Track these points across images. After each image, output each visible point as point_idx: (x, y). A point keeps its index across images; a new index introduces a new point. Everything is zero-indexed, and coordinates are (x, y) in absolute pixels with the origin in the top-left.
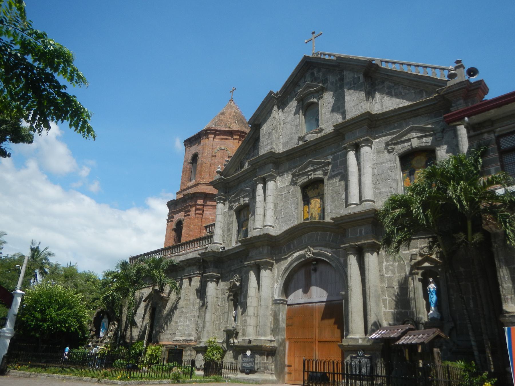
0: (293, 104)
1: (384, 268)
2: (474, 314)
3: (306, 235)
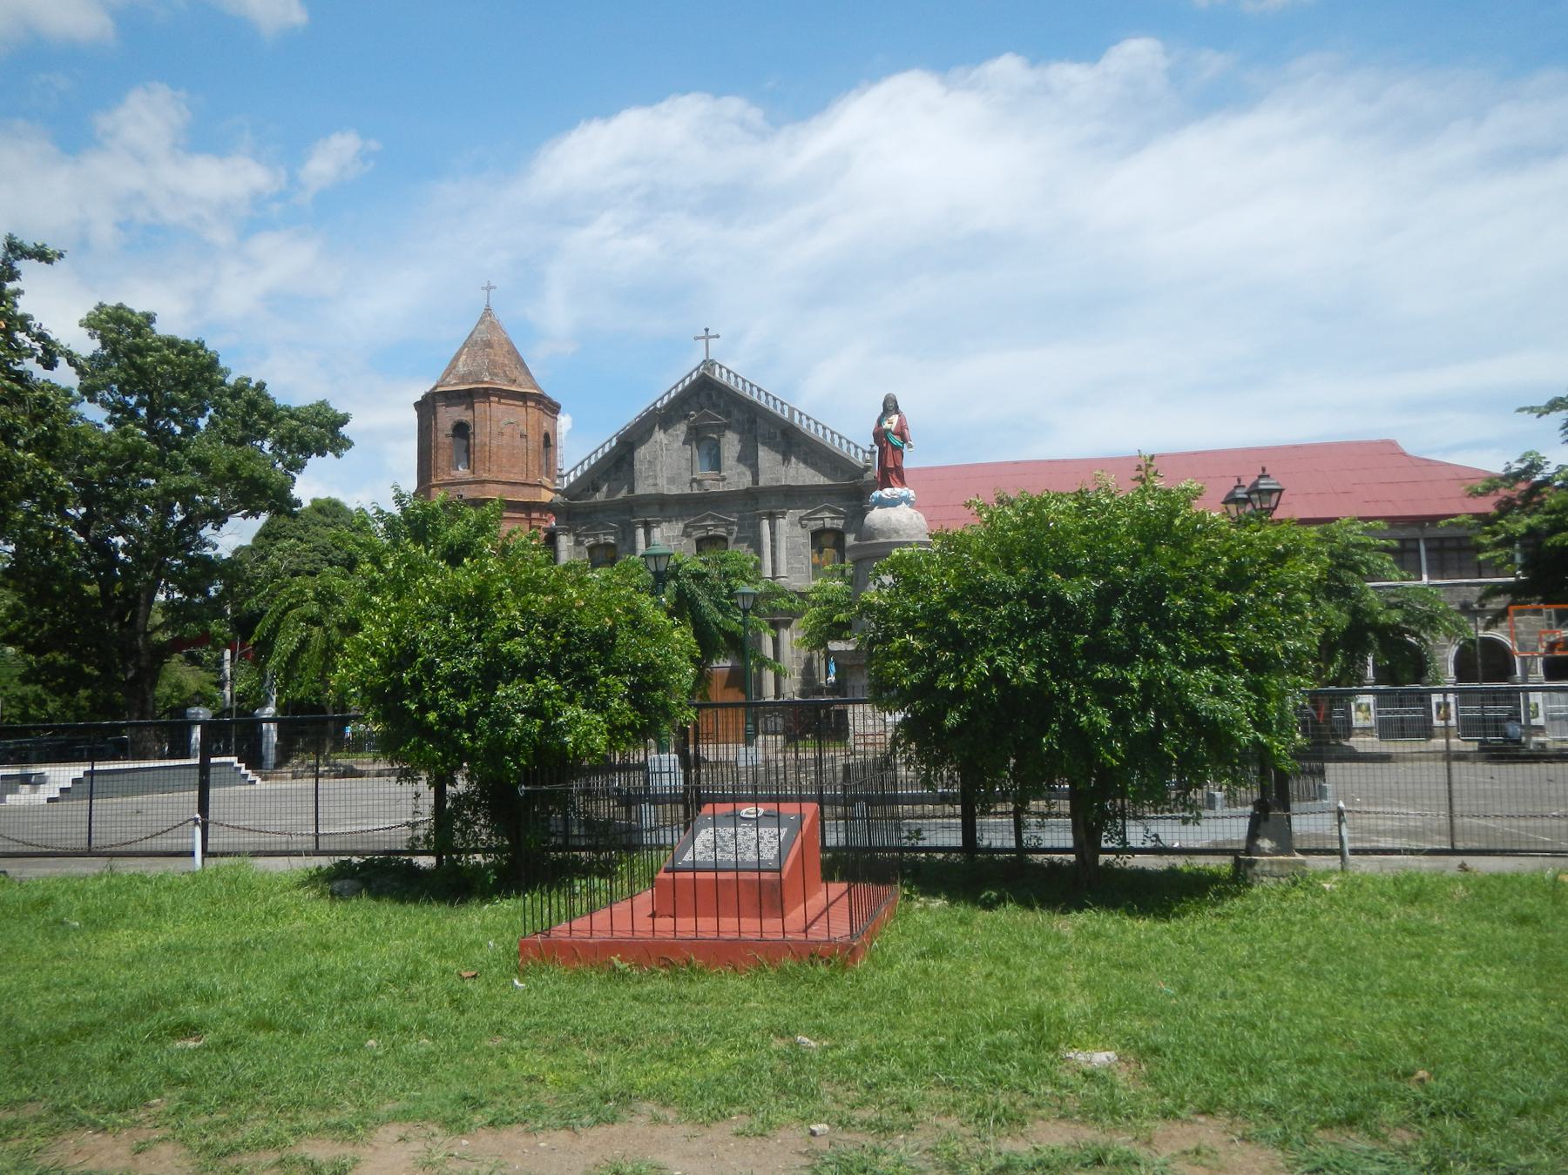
0: (681, 429)
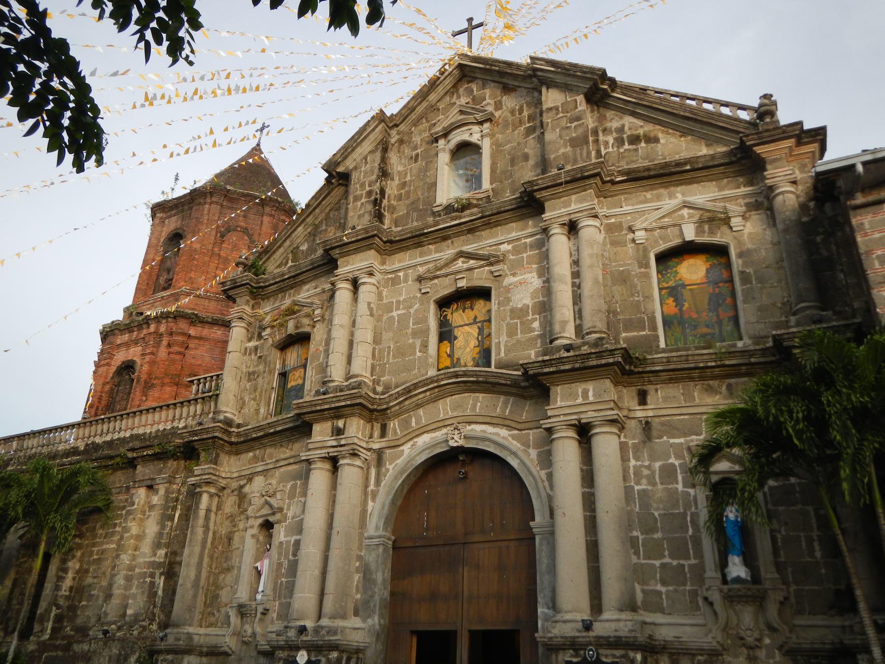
1: (631, 471)
2: (823, 571)
3: (448, 399)
